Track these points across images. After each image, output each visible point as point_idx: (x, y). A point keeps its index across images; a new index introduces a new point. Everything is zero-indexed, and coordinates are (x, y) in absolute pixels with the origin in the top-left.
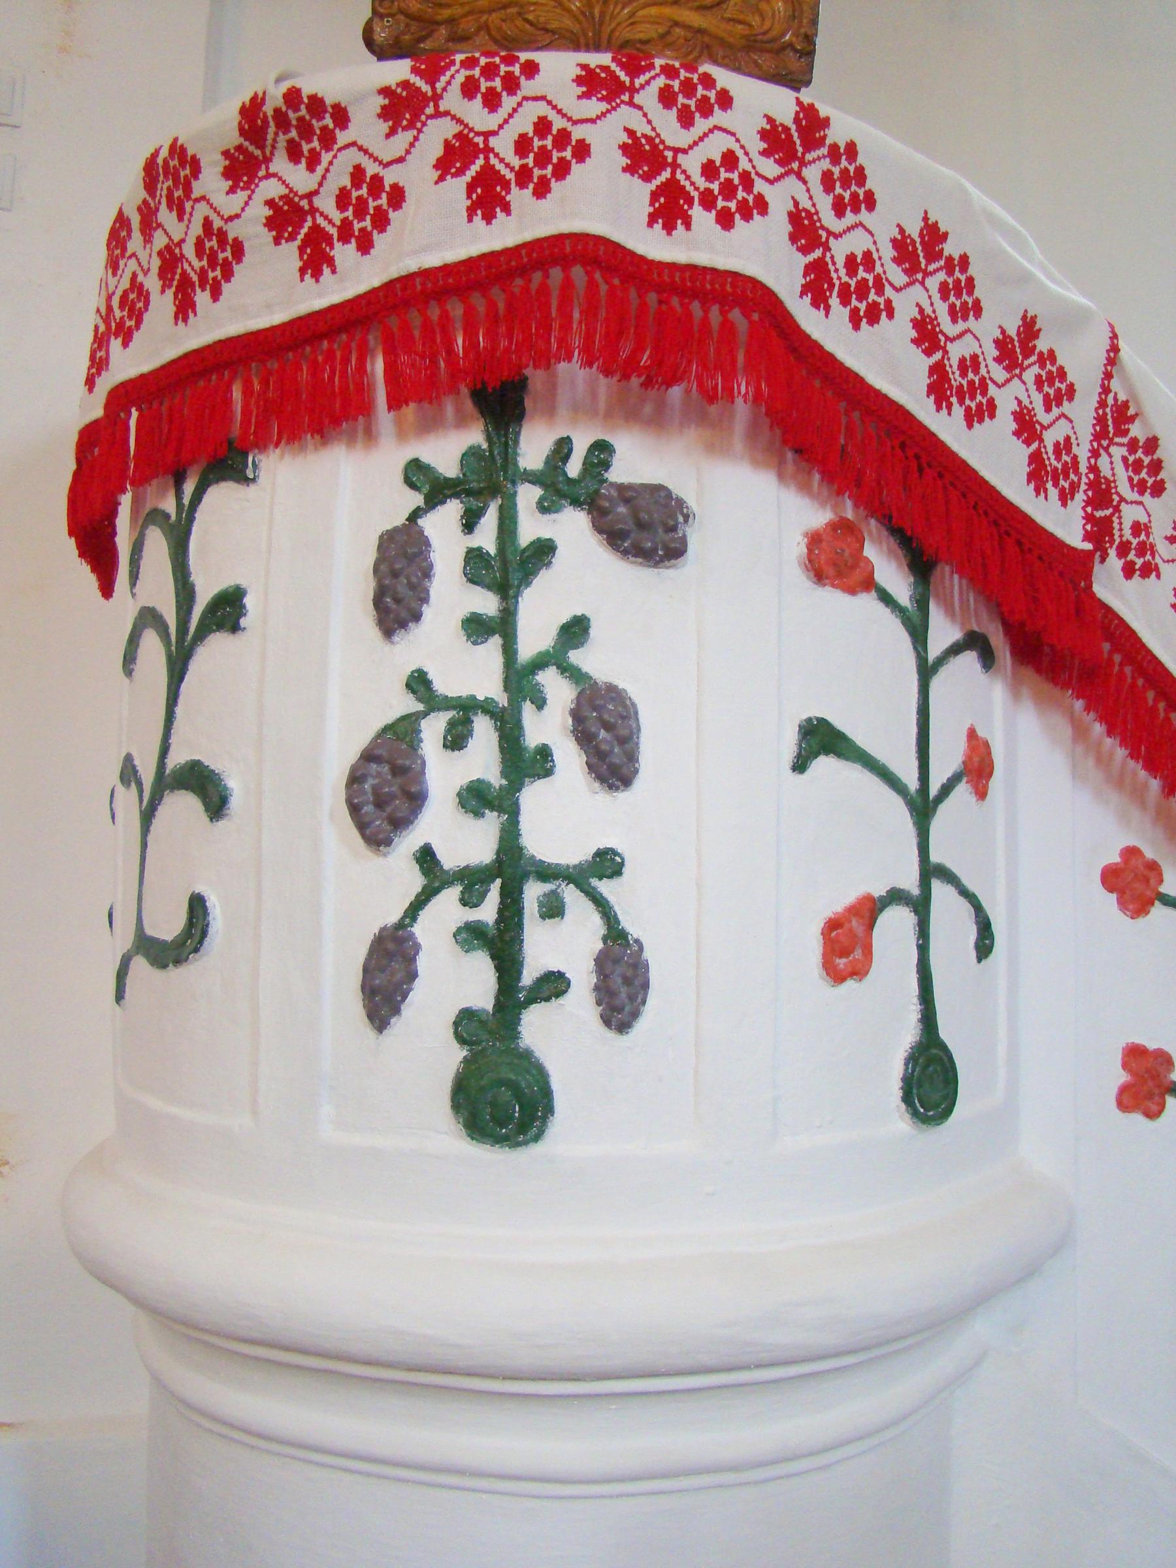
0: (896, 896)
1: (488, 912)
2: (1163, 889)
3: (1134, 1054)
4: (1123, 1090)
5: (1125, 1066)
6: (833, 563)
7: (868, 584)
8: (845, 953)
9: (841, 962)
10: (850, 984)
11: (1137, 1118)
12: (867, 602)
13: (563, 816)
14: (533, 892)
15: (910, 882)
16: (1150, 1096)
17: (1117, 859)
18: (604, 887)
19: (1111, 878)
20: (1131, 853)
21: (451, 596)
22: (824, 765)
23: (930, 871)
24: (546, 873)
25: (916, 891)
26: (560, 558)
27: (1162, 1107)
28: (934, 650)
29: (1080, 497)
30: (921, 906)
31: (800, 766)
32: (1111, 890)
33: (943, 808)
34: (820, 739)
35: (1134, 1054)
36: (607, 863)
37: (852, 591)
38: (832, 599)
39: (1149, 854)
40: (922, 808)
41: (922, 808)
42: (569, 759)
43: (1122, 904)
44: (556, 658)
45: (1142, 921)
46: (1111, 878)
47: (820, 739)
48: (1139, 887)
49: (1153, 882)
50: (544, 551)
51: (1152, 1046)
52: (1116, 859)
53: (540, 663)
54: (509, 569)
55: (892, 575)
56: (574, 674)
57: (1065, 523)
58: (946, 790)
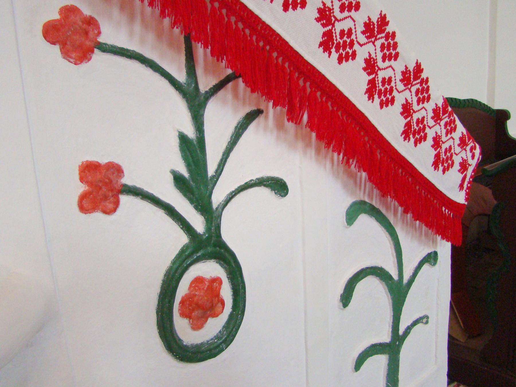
2: (101, 39)
3: (89, 170)
4: (83, 197)
11: (98, 216)
16: (105, 198)
17: (57, 17)
19: (52, 32)
20: (69, 11)
27: (117, 204)
35: (89, 170)
39: (87, 11)
43: (66, 54)
45: (85, 66)
46: (52, 32)
48: (78, 39)
49: (91, 35)
51: (103, 160)
52: (56, 16)
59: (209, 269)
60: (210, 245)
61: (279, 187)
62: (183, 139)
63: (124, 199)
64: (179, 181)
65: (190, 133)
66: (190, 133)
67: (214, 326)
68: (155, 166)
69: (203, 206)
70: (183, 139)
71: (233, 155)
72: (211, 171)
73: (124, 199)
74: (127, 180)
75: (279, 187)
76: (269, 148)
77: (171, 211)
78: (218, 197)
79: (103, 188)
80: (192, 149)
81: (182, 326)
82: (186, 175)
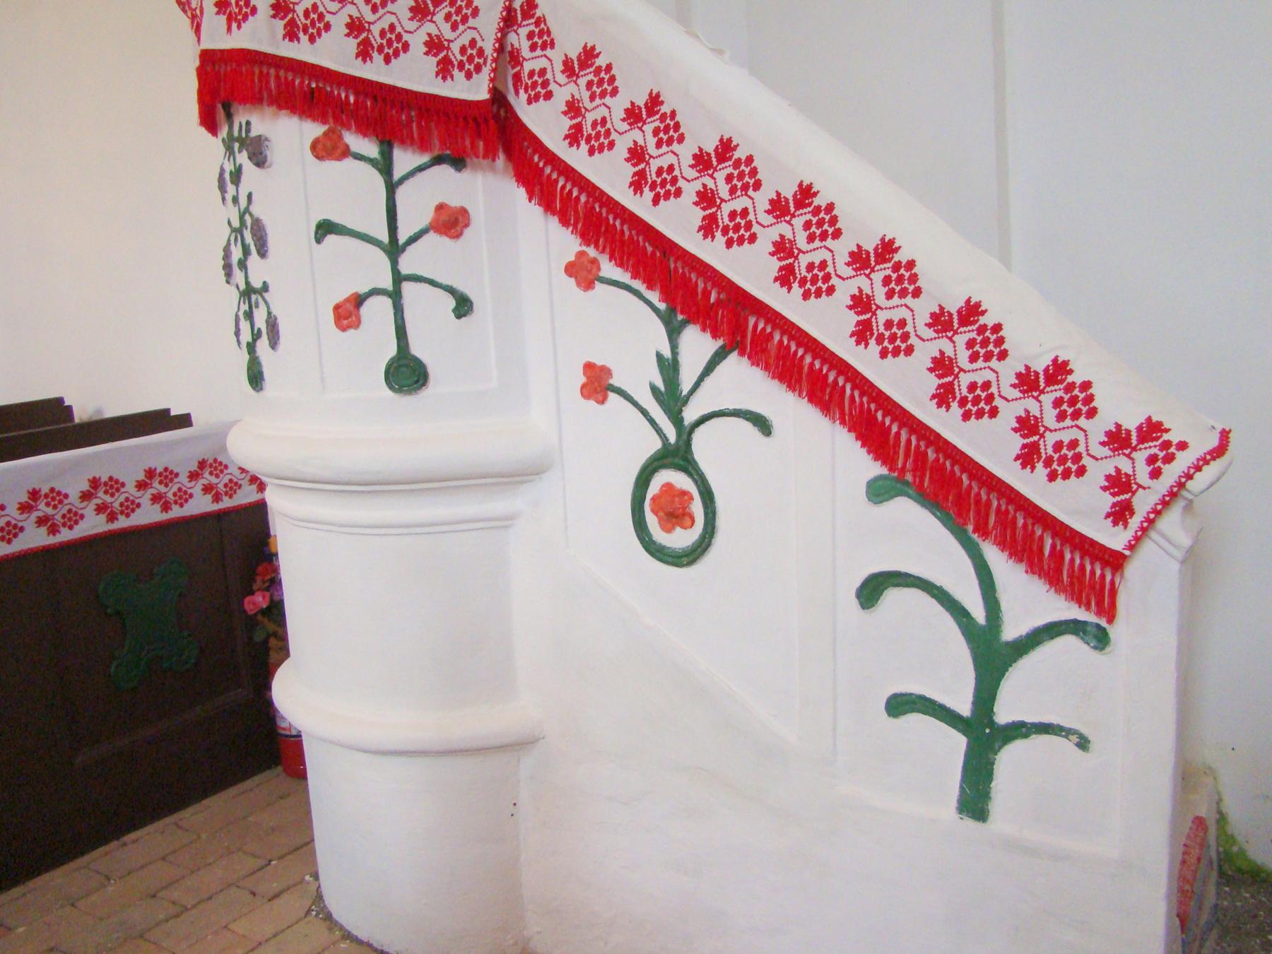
0: (376, 292)
1: (246, 307)
2: (601, 274)
3: (589, 367)
5: (585, 373)
6: (328, 149)
7: (346, 153)
8: (346, 318)
9: (345, 322)
10: (351, 331)
12: (349, 162)
13: (258, 271)
14: (254, 297)
15: (387, 283)
18: (266, 295)
19: (571, 269)
21: (231, 189)
22: (331, 239)
23: (398, 278)
24: (255, 291)
25: (391, 288)
26: (244, 168)
28: (398, 174)
29: (486, 70)
30: (396, 296)
31: (319, 241)
32: (570, 276)
33: (410, 249)
34: (326, 229)
35: (589, 367)
36: (265, 287)
37: (339, 159)
38: (332, 166)
40: (394, 249)
41: (394, 249)
42: (253, 248)
43: (579, 284)
44: (247, 210)
45: (590, 293)
46: (571, 269)
47: (326, 229)
49: (594, 270)
50: (241, 166)
51: (599, 363)
52: (573, 258)
53: (244, 213)
54: (237, 176)
55: (369, 148)
56: (251, 215)
57: (475, 90)
58: (413, 239)
59: (681, 481)
60: (677, 455)
61: (762, 425)
62: (659, 356)
63: (612, 396)
64: (654, 389)
65: (667, 353)
66: (667, 353)
67: (681, 539)
68: (638, 375)
69: (677, 420)
70: (659, 356)
71: (708, 381)
72: (686, 387)
73: (612, 396)
74: (615, 381)
75: (762, 425)
76: (742, 382)
77: (644, 413)
78: (690, 415)
79: (597, 383)
80: (669, 367)
81: (652, 520)
82: (662, 388)
